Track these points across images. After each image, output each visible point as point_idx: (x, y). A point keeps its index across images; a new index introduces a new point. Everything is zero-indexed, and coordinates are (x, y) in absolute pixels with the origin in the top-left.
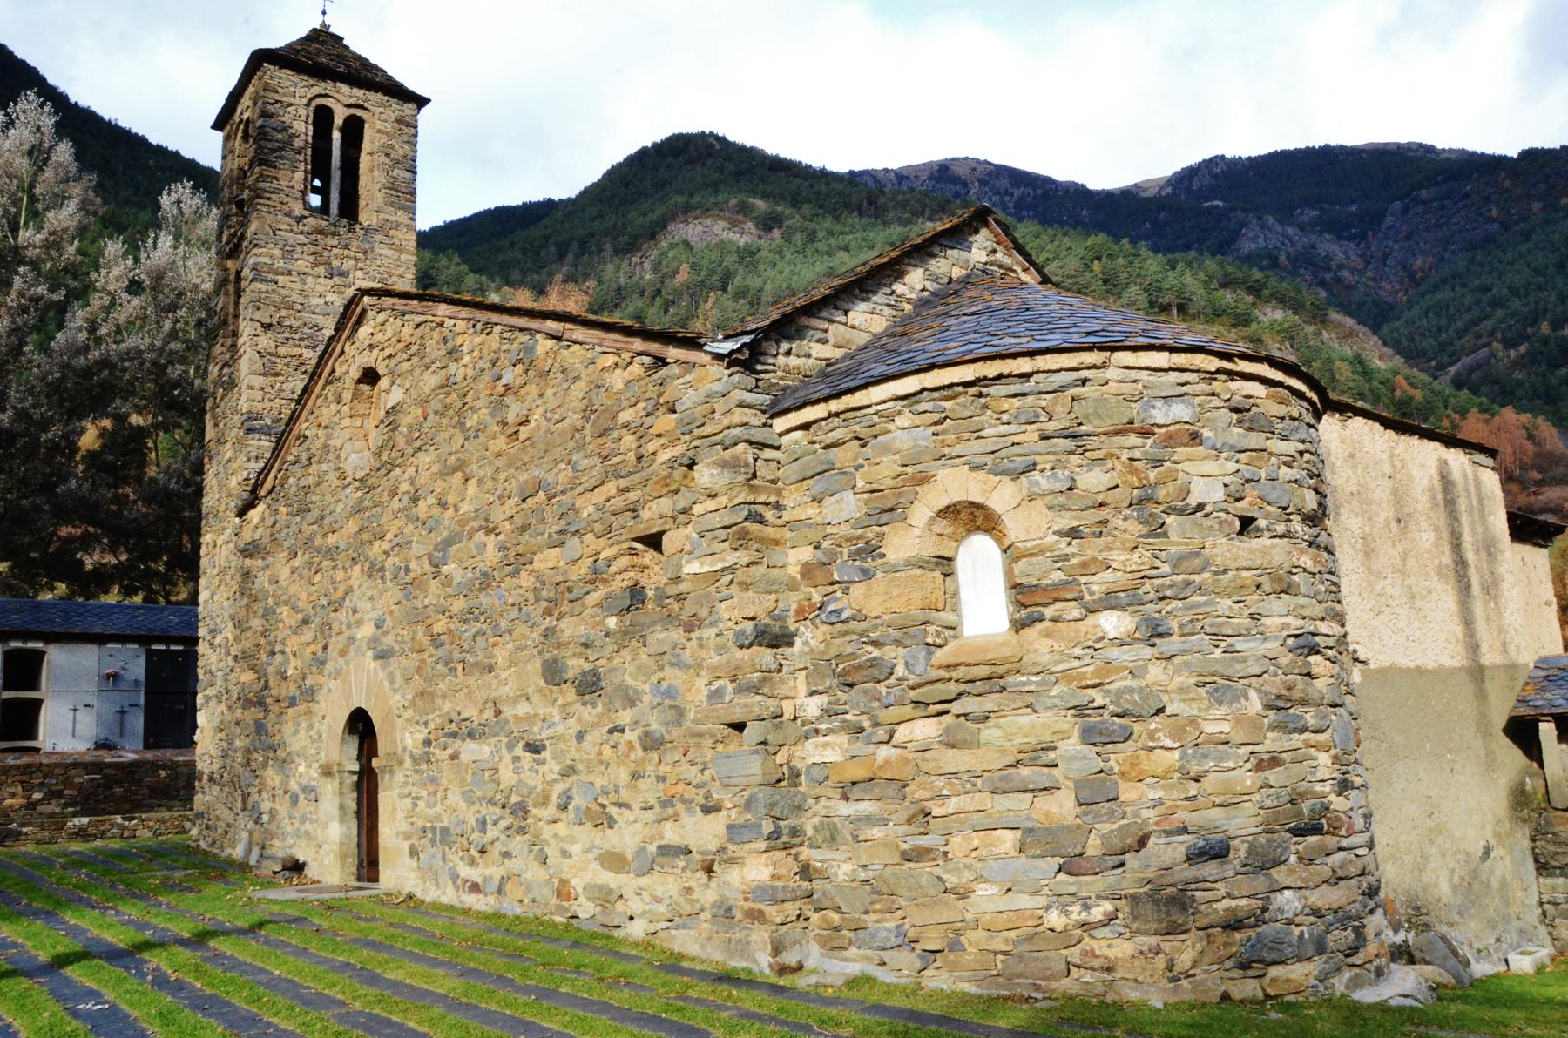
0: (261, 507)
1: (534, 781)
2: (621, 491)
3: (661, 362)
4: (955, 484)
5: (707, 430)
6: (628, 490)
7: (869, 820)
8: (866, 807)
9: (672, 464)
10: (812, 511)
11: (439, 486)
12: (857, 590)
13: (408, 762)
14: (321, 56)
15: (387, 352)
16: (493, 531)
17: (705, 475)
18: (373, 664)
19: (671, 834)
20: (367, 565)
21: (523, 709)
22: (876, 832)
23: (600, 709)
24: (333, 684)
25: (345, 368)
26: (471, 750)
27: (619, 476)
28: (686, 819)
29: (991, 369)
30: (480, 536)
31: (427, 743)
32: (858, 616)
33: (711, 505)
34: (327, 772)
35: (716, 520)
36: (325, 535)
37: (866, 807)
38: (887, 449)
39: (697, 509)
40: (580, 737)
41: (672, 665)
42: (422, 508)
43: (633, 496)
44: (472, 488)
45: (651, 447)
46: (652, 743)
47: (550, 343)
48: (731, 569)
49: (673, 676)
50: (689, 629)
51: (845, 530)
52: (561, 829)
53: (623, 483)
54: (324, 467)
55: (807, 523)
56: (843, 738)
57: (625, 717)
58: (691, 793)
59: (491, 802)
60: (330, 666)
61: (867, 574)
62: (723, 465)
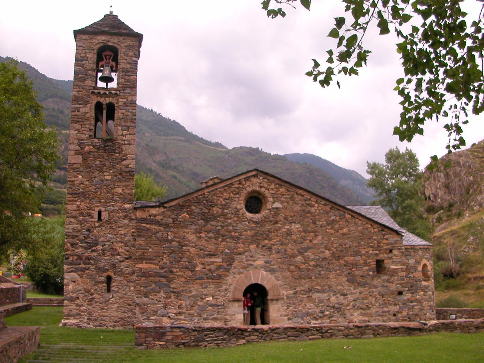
0: (162, 210)
1: (345, 302)
2: (373, 250)
3: (383, 230)
4: (424, 261)
5: (396, 245)
6: (376, 250)
7: (416, 305)
8: (415, 304)
9: (387, 249)
10: (407, 261)
11: (303, 234)
12: (414, 274)
13: (285, 298)
14: (111, 26)
15: (272, 192)
16: (329, 250)
17: (395, 252)
18: (265, 272)
19: (385, 309)
20: (260, 246)
21: (339, 288)
22: (416, 307)
23: (366, 288)
24: (238, 276)
25: (241, 186)
26: (315, 296)
27: (372, 247)
28: (389, 306)
29: (428, 247)
30: (324, 250)
31: (296, 293)
32: (414, 277)
33: (397, 258)
34: (238, 301)
35: (398, 260)
36: (230, 232)
37: (415, 304)
38: (418, 254)
39: (393, 258)
40: (360, 293)
41: (386, 282)
42: (294, 237)
43: (377, 252)
44: (320, 238)
45: (382, 244)
46: (380, 294)
47: (350, 216)
48: (401, 269)
49: (386, 284)
50: (391, 277)
51: (412, 265)
52: (351, 311)
53: (374, 249)
54: (226, 211)
55: (406, 262)
56: (411, 295)
57: (374, 290)
58: (390, 302)
59: (328, 306)
60: (233, 270)
61: (416, 271)
62: (400, 252)
